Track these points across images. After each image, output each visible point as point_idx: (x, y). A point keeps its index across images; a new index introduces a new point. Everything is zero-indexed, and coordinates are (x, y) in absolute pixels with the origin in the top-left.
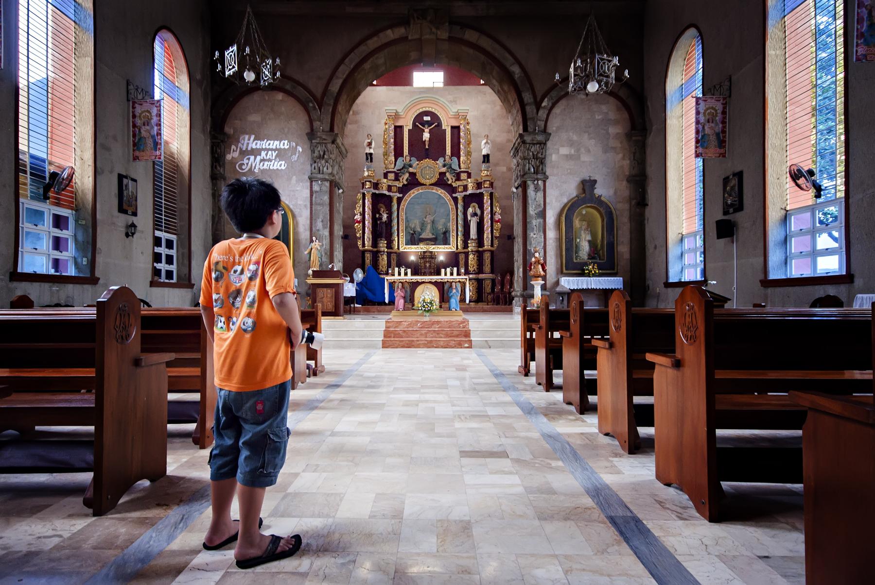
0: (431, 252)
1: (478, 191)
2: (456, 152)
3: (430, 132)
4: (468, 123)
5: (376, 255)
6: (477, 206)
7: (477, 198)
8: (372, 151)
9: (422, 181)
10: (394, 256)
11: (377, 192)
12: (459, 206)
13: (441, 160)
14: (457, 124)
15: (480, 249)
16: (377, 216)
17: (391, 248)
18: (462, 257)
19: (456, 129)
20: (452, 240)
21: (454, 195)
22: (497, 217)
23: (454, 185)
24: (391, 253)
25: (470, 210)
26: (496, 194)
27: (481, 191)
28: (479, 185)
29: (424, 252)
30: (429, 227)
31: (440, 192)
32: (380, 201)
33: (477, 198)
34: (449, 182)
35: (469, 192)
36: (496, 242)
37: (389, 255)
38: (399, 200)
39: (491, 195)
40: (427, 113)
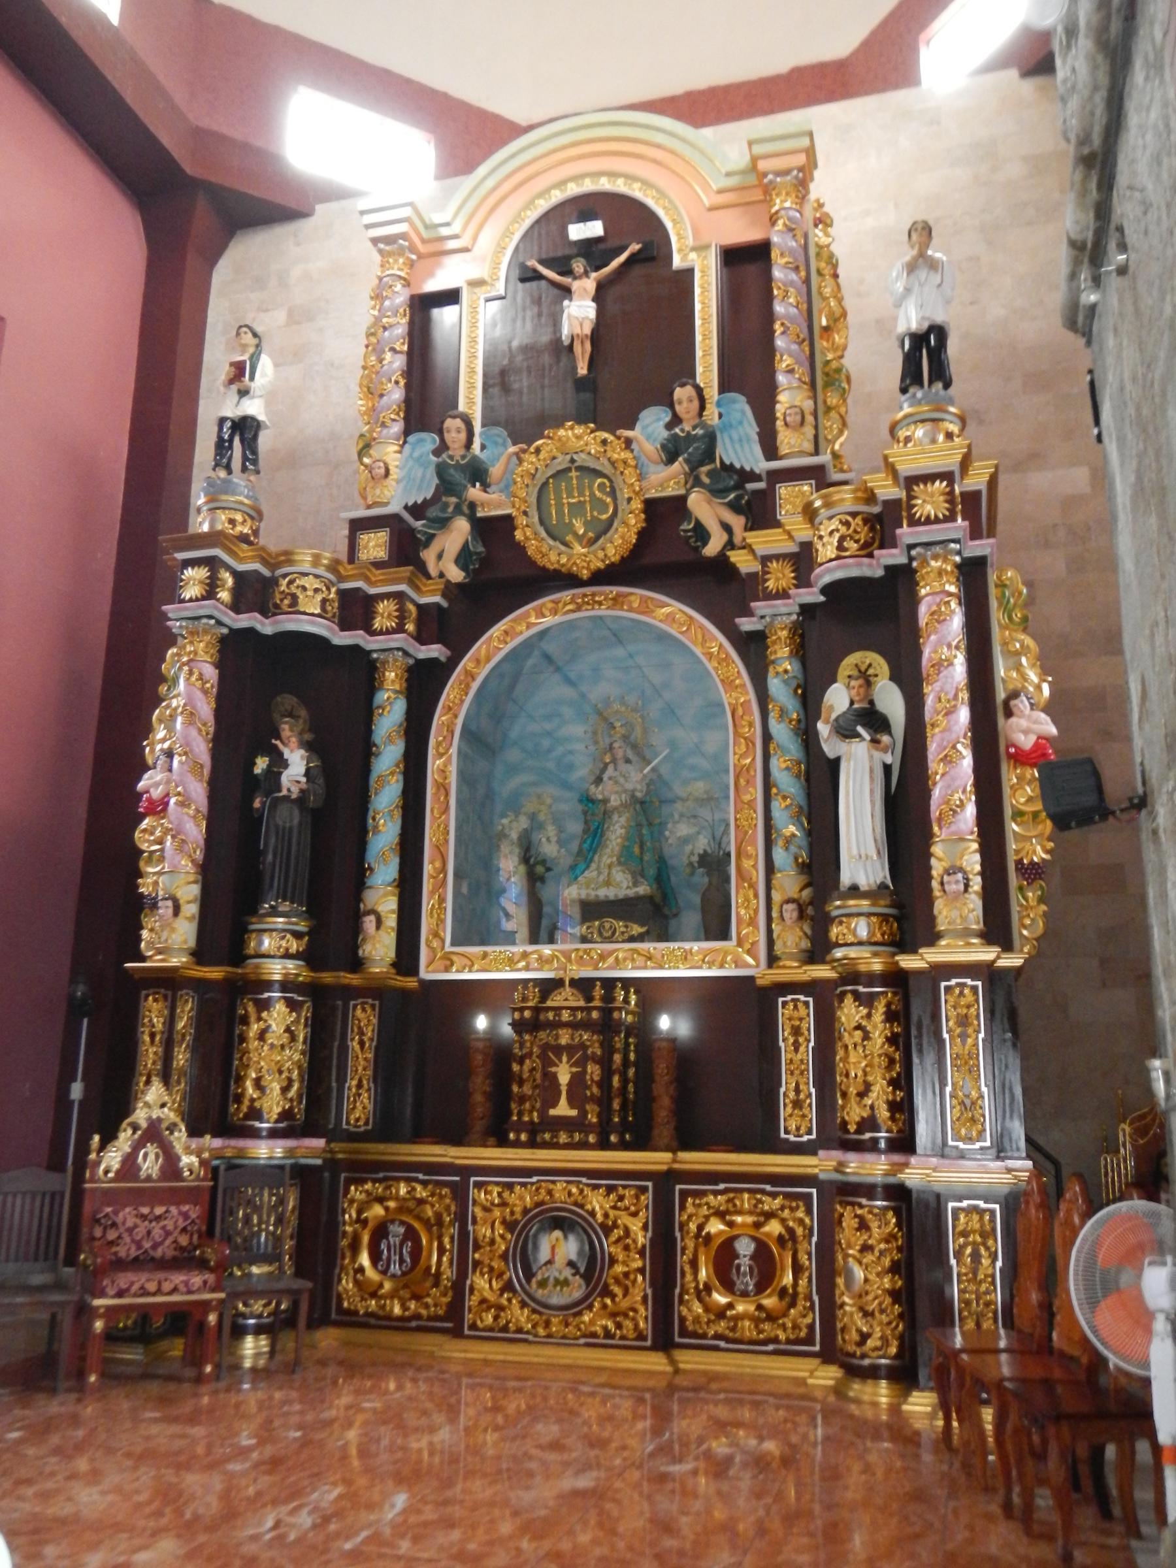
0: (584, 986)
1: (872, 568)
2: (748, 369)
3: (599, 297)
4: (823, 221)
5: (224, 1010)
6: (879, 665)
7: (873, 612)
8: (253, 407)
9: (553, 556)
10: (365, 1020)
11: (267, 627)
12: (775, 685)
13: (652, 426)
14: (751, 235)
15: (908, 962)
16: (261, 764)
17: (357, 964)
18: (795, 1015)
19: (746, 262)
20: (744, 905)
21: (746, 624)
22: (1029, 726)
23: (743, 562)
24: (349, 993)
25: (838, 698)
26: (1006, 578)
27: (894, 557)
28: (882, 523)
29: (548, 987)
30: (617, 832)
31: (670, 613)
32: (266, 676)
33: (873, 612)
34: (712, 549)
35: (825, 575)
36: (1029, 913)
37: (323, 1010)
38: (425, 684)
39: (972, 573)
40: (585, 207)
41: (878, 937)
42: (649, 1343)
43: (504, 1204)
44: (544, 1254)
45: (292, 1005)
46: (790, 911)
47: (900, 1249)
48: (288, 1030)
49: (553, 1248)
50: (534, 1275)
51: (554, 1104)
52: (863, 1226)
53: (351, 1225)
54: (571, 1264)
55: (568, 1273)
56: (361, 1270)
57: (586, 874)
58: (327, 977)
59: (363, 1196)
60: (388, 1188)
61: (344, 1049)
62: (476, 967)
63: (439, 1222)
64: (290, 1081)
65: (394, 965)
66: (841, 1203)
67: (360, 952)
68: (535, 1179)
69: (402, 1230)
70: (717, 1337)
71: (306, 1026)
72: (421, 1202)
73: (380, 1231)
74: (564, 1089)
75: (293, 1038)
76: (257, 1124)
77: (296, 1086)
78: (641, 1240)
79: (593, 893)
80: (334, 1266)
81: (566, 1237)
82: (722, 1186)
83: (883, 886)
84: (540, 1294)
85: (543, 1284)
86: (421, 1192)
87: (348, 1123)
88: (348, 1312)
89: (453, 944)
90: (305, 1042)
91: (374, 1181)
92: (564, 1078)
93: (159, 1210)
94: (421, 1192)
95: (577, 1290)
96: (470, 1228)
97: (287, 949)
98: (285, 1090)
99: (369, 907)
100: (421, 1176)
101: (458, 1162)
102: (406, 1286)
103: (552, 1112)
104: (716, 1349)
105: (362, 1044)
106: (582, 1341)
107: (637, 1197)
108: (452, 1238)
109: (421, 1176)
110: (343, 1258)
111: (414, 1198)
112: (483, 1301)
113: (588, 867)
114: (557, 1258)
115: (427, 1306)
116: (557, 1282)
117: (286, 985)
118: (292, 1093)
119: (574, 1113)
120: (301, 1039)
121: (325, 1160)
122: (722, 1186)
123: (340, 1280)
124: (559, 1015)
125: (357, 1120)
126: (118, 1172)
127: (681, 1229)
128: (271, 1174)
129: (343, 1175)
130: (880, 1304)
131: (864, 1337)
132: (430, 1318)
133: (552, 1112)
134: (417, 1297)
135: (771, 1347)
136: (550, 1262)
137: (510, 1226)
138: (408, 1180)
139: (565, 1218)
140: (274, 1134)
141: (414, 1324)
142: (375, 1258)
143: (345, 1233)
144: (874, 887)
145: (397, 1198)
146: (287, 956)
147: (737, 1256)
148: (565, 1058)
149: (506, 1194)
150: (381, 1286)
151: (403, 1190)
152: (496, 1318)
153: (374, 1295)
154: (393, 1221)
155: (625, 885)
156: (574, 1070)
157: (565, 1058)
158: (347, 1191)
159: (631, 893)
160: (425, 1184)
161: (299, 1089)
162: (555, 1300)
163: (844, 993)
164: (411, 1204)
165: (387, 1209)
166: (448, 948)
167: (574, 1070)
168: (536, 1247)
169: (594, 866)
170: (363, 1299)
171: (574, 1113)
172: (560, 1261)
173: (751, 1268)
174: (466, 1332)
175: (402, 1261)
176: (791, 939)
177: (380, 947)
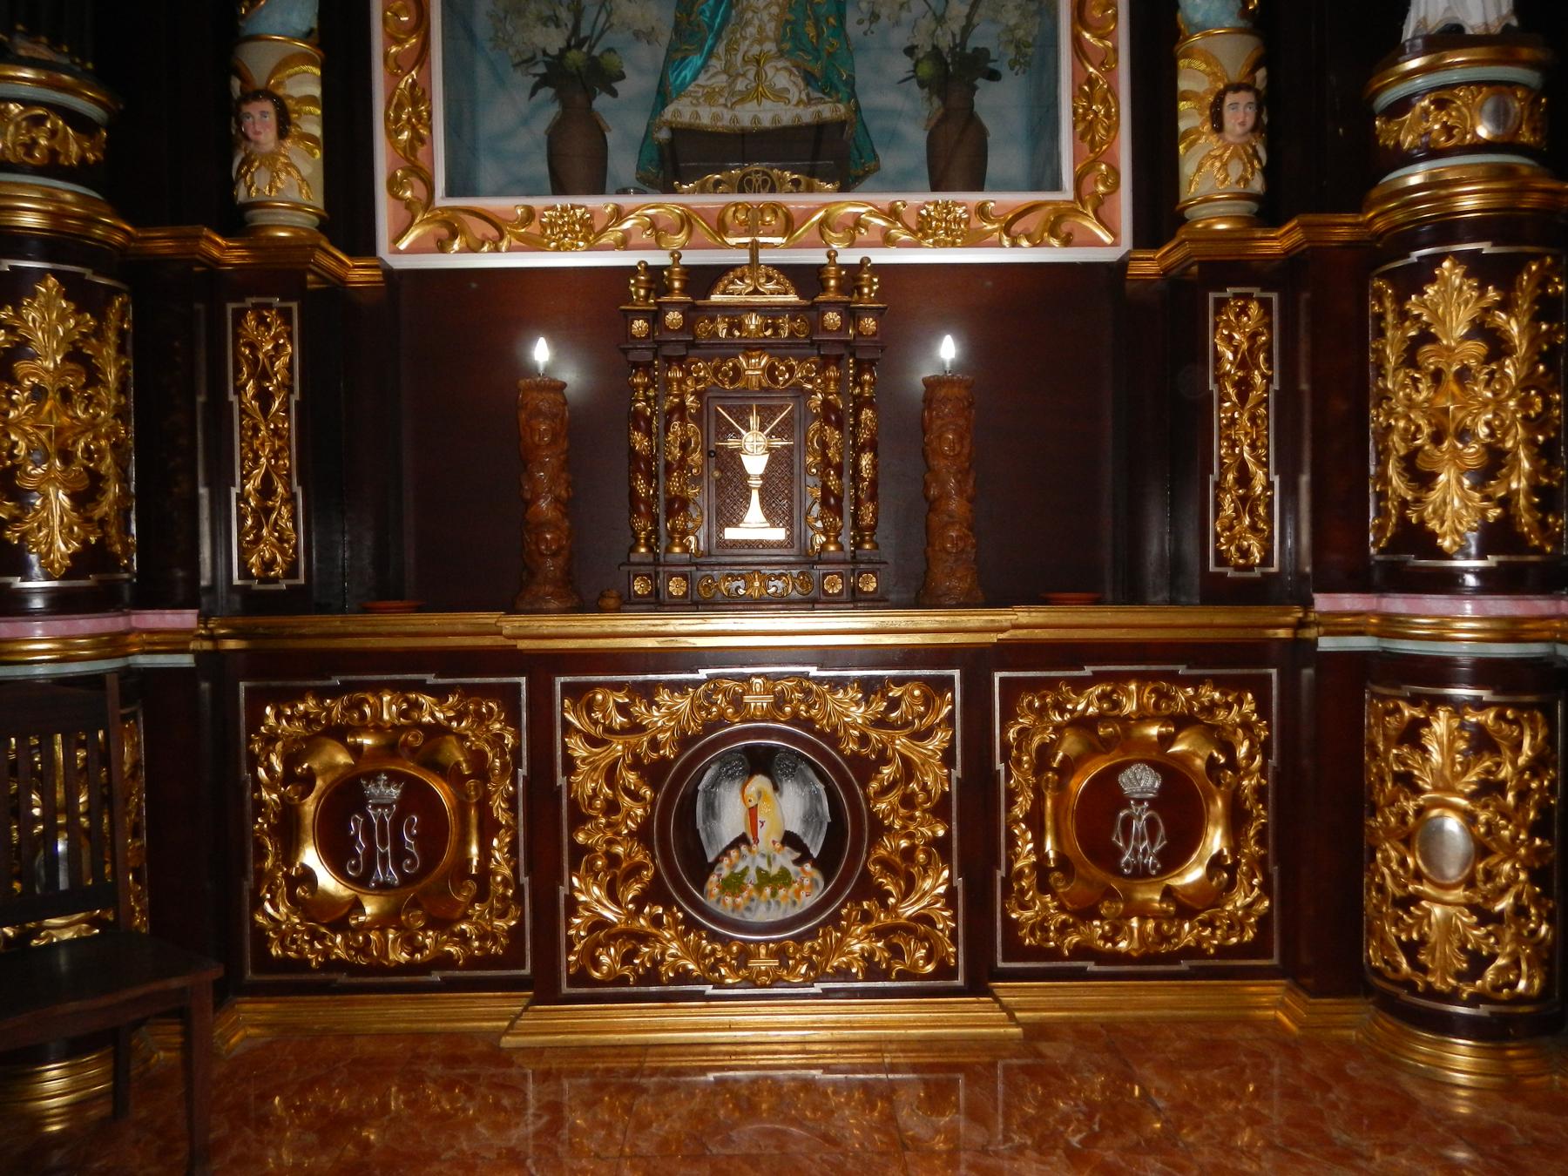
41: (1526, 137)
42: (960, 982)
43: (636, 728)
44: (731, 822)
45: (79, 294)
46: (1239, 113)
48: (75, 355)
49: (753, 812)
50: (711, 867)
51: (735, 521)
53: (272, 788)
54: (790, 840)
55: (786, 859)
56: (308, 876)
57: (702, 80)
58: (162, 242)
60: (357, 705)
61: (219, 412)
62: (504, 245)
63: (481, 769)
64: (96, 478)
65: (325, 226)
66: (1414, 701)
67: (241, 194)
68: (703, 674)
69: (394, 792)
70: (1081, 952)
71: (121, 350)
72: (436, 731)
73: (346, 796)
74: (755, 483)
75: (93, 377)
76: (18, 583)
78: (936, 790)
79: (727, 115)
80: (243, 873)
81: (776, 788)
82: (1088, 671)
83: (1507, 28)
84: (725, 905)
85: (734, 884)
86: (431, 711)
87: (245, 572)
88: (284, 964)
89: (450, 192)
90: (122, 389)
91: (320, 695)
92: (755, 464)
94: (431, 711)
95: (808, 888)
96: (561, 780)
97: (53, 153)
98: (83, 499)
99: (259, 83)
100: (431, 679)
101: (523, 644)
102: (415, 904)
103: (731, 534)
104: (1081, 975)
105: (264, 398)
106: (817, 988)
107: (928, 701)
108: (512, 800)
109: (431, 679)
110: (261, 855)
111: (419, 725)
112: (600, 924)
113: (704, 66)
114: (761, 833)
115: (464, 939)
116: (764, 879)
117: (52, 244)
118: (104, 508)
119: (779, 534)
120: (112, 375)
121: (199, 655)
122: (1088, 671)
123: (258, 904)
124: (740, 326)
125: (268, 565)
127: (1005, 757)
128: (67, 703)
129: (242, 685)
130: (1518, 897)
131: (1479, 963)
132: (472, 962)
133: (731, 534)
134: (441, 923)
135: (1184, 965)
136: (742, 840)
137: (653, 772)
138: (400, 688)
139: (773, 750)
140: (61, 604)
141: (436, 977)
142: (336, 858)
143: (260, 803)
144: (1495, 29)
145: (378, 728)
146: (53, 168)
147: (1124, 802)
148: (754, 421)
149: (639, 709)
150: (357, 906)
151: (389, 708)
152: (627, 959)
153: (340, 925)
154: (372, 777)
155: (794, 95)
156: (778, 443)
157: (754, 421)
158: (257, 719)
159: (807, 115)
160: (440, 693)
161: (125, 492)
162: (762, 915)
163: (1437, 260)
164: (414, 739)
165: (356, 750)
166: (441, 200)
167: (778, 443)
168: (712, 811)
169: (717, 64)
170: (315, 936)
171: (779, 534)
172: (768, 836)
173: (1151, 823)
174: (565, 989)
175: (400, 854)
176: (1216, 173)
177: (285, 181)
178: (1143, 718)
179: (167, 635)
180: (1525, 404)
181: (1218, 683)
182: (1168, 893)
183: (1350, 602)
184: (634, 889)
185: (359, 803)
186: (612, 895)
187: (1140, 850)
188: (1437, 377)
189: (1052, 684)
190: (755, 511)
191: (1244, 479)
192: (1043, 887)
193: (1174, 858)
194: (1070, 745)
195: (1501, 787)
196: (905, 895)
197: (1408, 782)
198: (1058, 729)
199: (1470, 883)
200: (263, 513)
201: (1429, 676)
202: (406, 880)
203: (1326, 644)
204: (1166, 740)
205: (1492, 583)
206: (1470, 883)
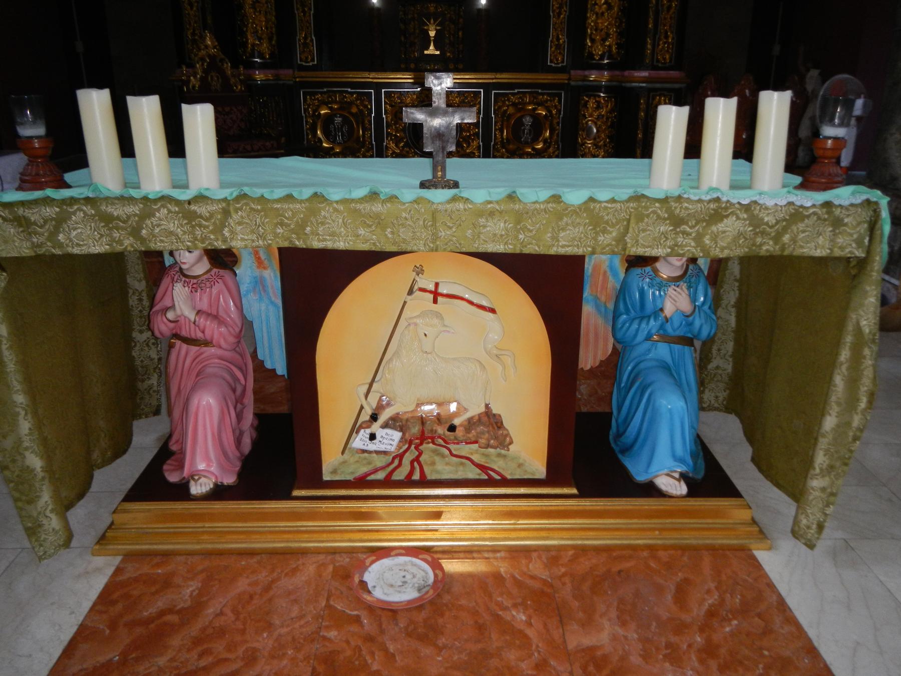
47: (615, 117)
51: (427, 49)
52: (599, 106)
59: (316, 102)
72: (351, 104)
73: (329, 119)
77: (275, 38)
82: (516, 91)
92: (432, 34)
93: (227, 109)
100: (349, 90)
103: (426, 52)
109: (349, 90)
119: (438, 53)
122: (516, 91)
126: (199, 87)
133: (426, 52)
147: (523, 125)
148: (432, 21)
157: (432, 21)
165: (331, 109)
171: (438, 53)
178: (529, 104)
179: (287, 74)
180: (616, 22)
181: (548, 94)
182: (534, 149)
183: (580, 72)
184: (402, 144)
185: (333, 122)
186: (396, 146)
187: (526, 136)
188: (597, 14)
189: (507, 94)
190: (432, 47)
191: (558, 39)
192: (503, 147)
193: (535, 140)
194: (511, 110)
195: (603, 116)
196: (468, 147)
197: (584, 115)
198: (508, 106)
199: (595, 139)
200: (305, 45)
201: (594, 89)
202: (345, 142)
203: (573, 83)
204: (534, 109)
205: (609, 67)
206: (595, 139)
